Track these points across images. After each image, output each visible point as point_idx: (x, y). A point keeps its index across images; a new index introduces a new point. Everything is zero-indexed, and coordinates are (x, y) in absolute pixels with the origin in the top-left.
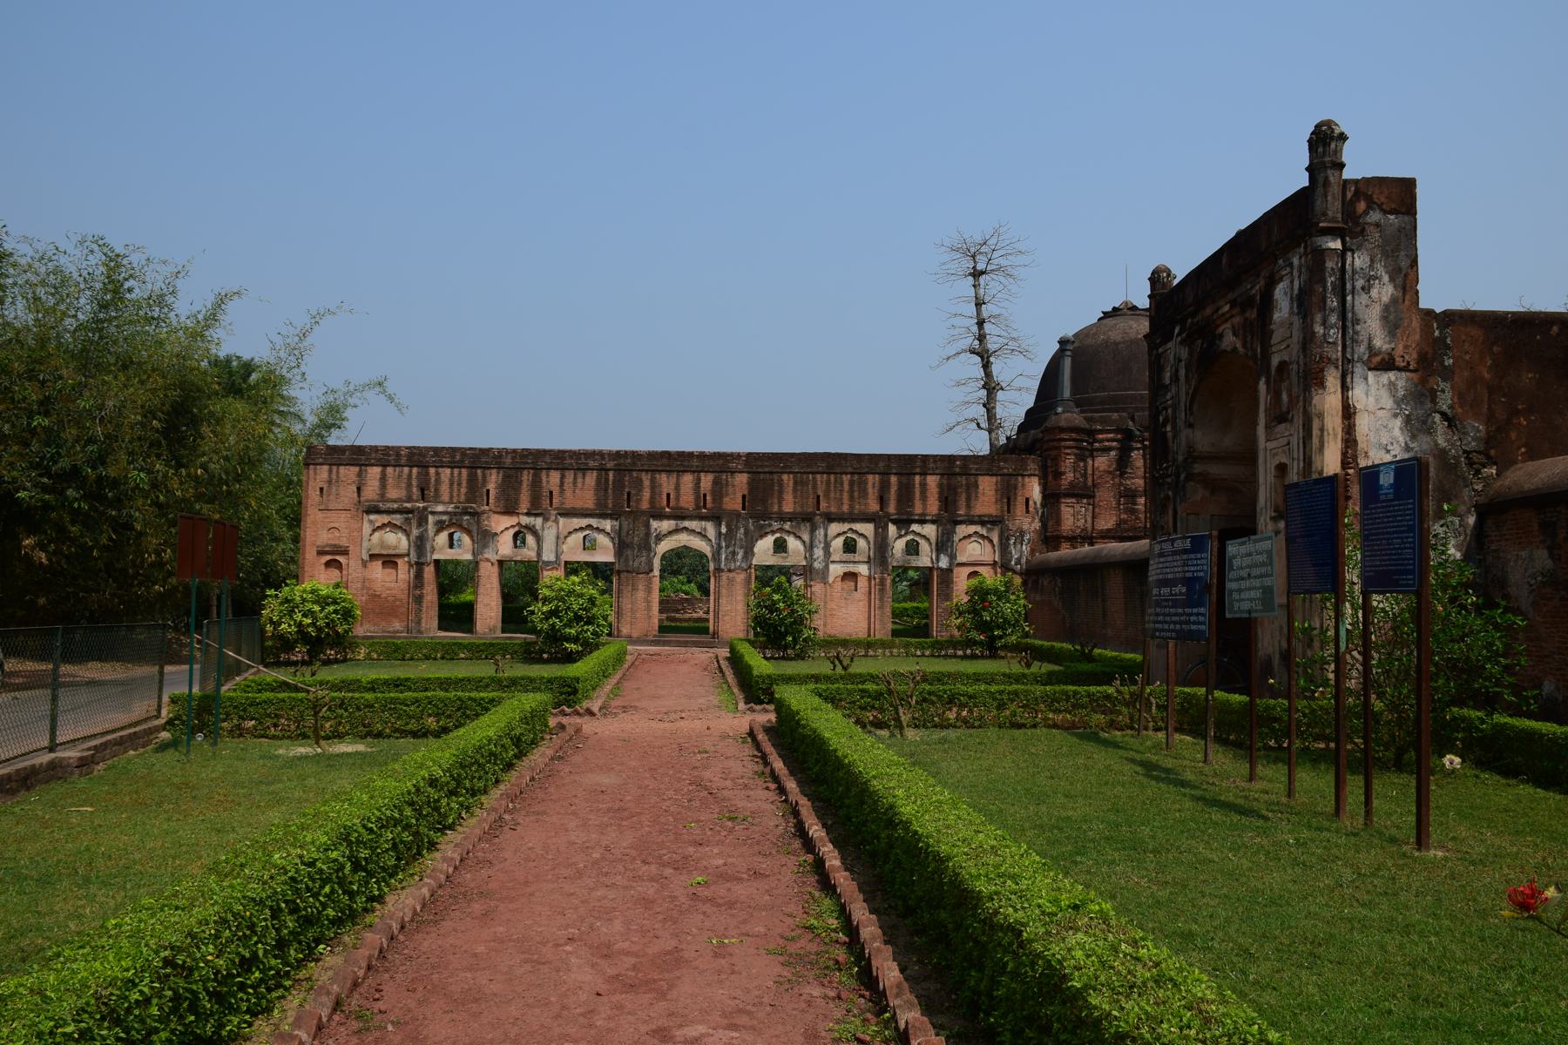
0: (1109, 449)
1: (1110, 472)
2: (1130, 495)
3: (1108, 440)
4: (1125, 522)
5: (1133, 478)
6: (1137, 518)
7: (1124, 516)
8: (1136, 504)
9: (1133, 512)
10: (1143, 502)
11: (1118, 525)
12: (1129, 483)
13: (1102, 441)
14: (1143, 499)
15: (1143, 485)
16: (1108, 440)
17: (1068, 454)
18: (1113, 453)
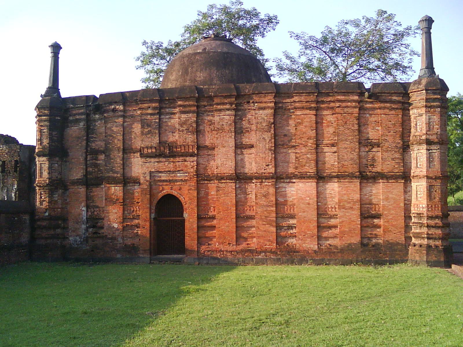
0: (77, 121)
1: (79, 138)
2: (96, 153)
3: (79, 114)
4: (91, 173)
5: (96, 141)
6: (99, 170)
7: (90, 169)
8: (97, 160)
9: (96, 165)
10: (103, 158)
11: (86, 175)
12: (94, 145)
13: (75, 115)
14: (104, 155)
15: (104, 146)
16: (79, 114)
17: (41, 126)
18: (82, 124)
